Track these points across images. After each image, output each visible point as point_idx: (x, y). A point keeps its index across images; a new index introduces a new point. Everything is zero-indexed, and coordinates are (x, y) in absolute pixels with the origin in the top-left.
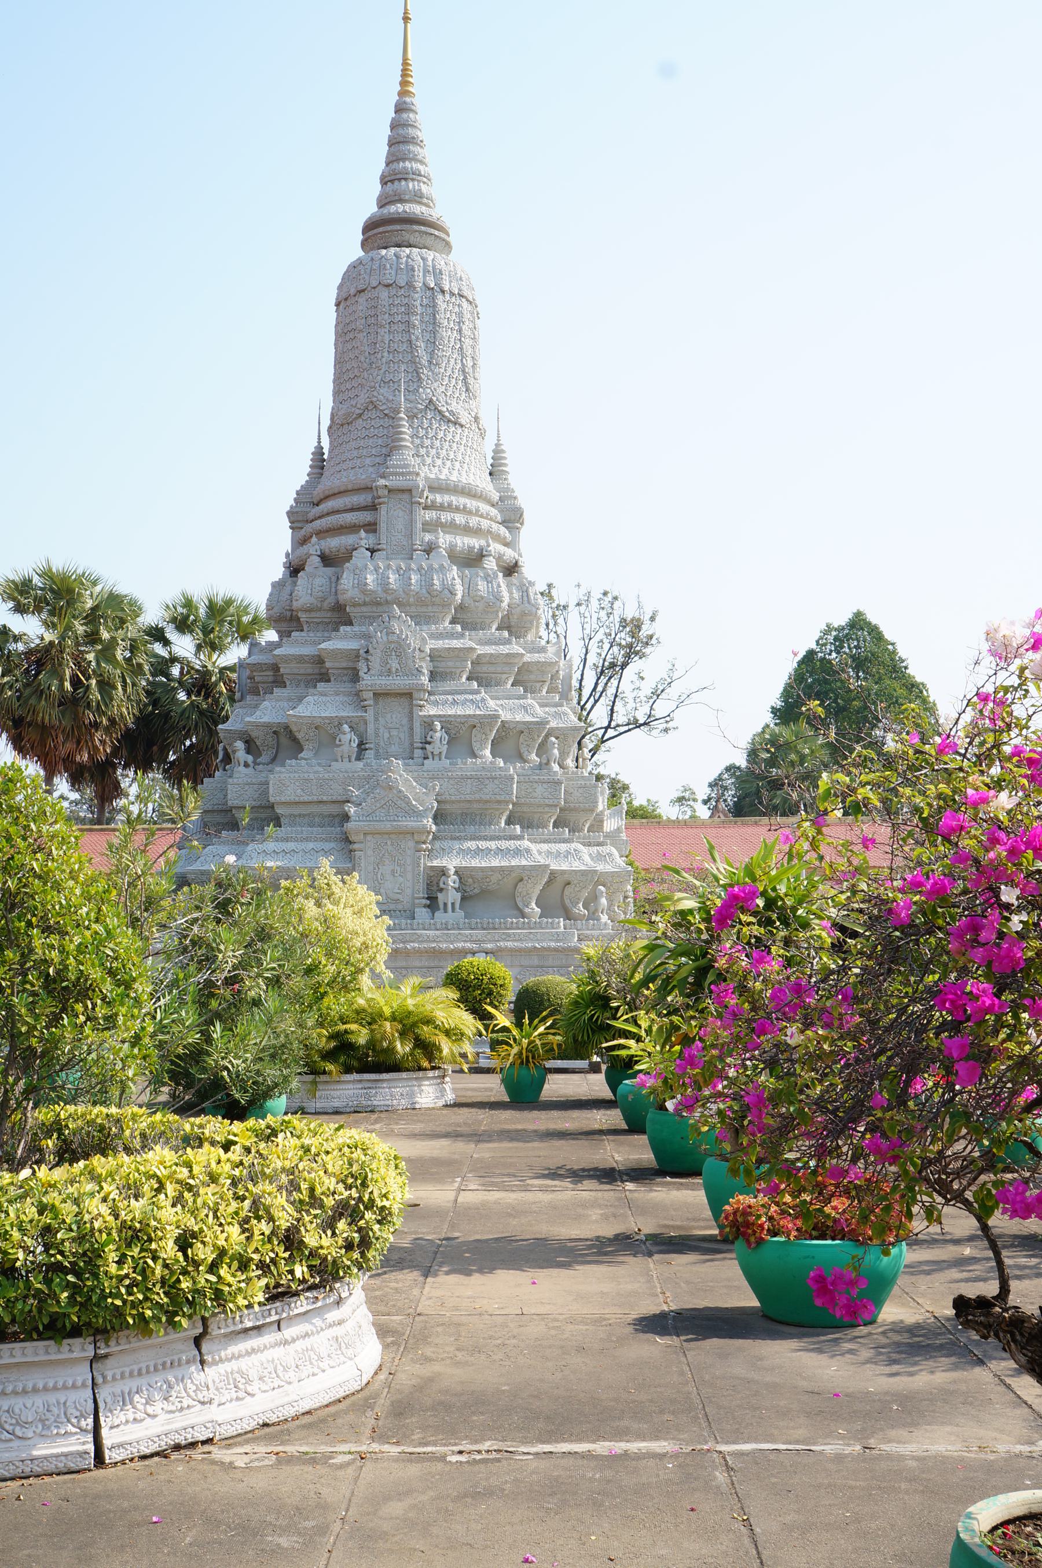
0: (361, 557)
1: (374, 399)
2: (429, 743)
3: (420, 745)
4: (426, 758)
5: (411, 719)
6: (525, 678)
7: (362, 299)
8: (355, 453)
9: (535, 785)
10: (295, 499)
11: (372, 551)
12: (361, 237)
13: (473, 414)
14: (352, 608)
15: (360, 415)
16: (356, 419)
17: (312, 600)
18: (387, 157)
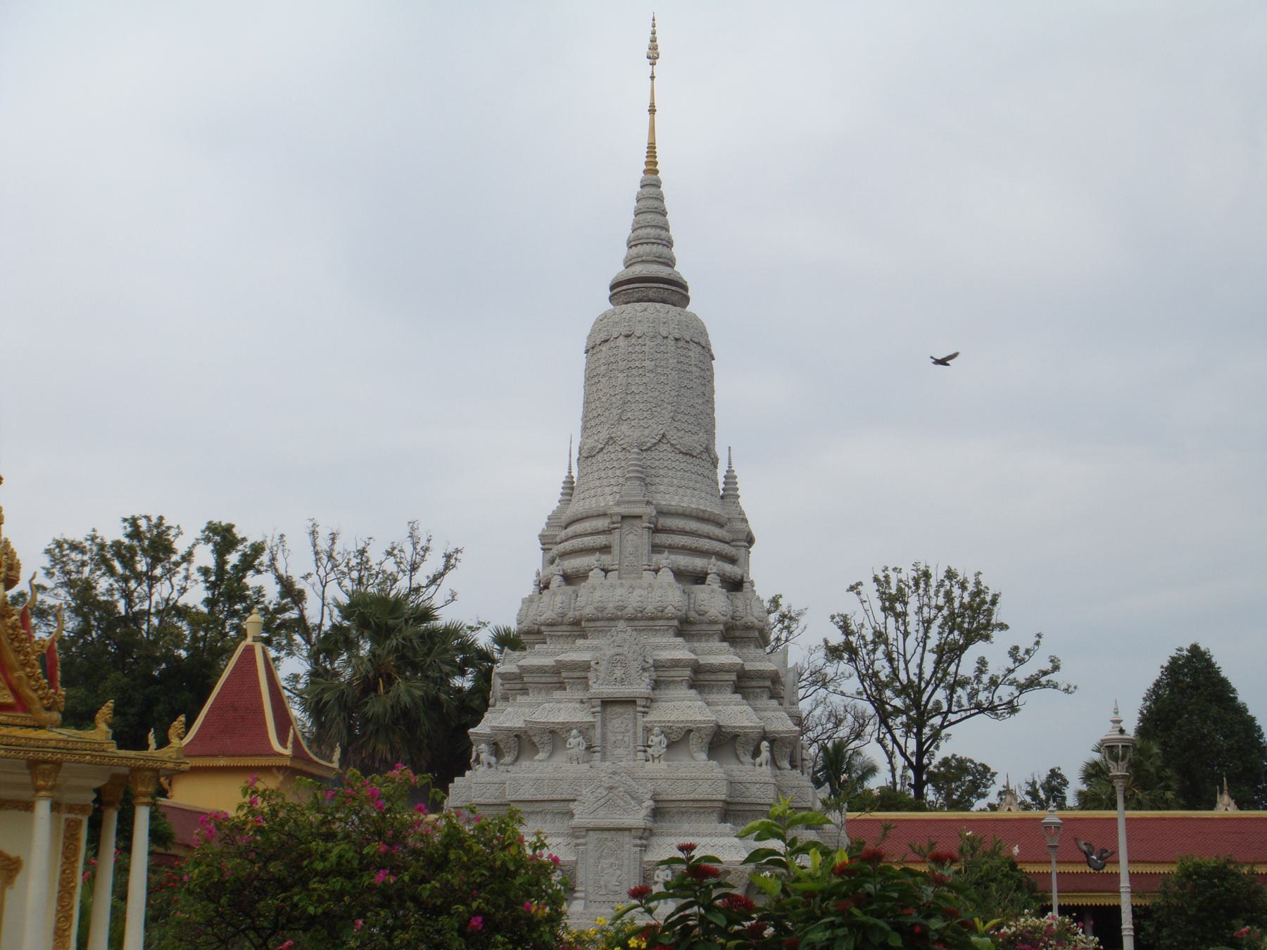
0: (596, 576)
1: (613, 435)
2: (650, 746)
3: (643, 748)
4: (647, 760)
5: (635, 725)
6: (748, 684)
7: (604, 348)
8: (597, 483)
9: (748, 785)
10: (547, 524)
11: (606, 571)
12: (609, 293)
13: (704, 446)
14: (587, 623)
15: (602, 449)
16: (598, 452)
17: (554, 616)
18: (633, 225)
